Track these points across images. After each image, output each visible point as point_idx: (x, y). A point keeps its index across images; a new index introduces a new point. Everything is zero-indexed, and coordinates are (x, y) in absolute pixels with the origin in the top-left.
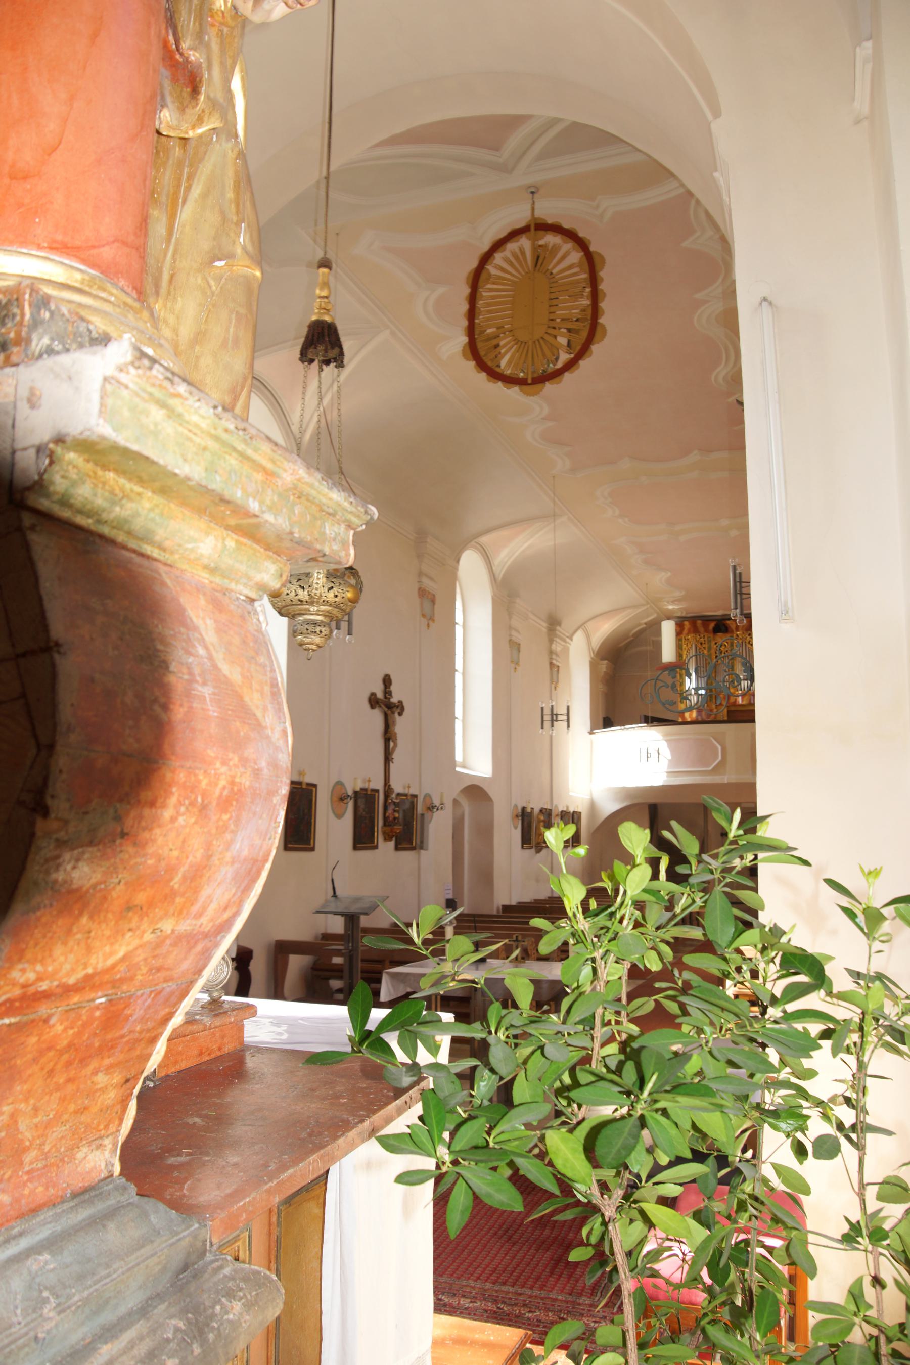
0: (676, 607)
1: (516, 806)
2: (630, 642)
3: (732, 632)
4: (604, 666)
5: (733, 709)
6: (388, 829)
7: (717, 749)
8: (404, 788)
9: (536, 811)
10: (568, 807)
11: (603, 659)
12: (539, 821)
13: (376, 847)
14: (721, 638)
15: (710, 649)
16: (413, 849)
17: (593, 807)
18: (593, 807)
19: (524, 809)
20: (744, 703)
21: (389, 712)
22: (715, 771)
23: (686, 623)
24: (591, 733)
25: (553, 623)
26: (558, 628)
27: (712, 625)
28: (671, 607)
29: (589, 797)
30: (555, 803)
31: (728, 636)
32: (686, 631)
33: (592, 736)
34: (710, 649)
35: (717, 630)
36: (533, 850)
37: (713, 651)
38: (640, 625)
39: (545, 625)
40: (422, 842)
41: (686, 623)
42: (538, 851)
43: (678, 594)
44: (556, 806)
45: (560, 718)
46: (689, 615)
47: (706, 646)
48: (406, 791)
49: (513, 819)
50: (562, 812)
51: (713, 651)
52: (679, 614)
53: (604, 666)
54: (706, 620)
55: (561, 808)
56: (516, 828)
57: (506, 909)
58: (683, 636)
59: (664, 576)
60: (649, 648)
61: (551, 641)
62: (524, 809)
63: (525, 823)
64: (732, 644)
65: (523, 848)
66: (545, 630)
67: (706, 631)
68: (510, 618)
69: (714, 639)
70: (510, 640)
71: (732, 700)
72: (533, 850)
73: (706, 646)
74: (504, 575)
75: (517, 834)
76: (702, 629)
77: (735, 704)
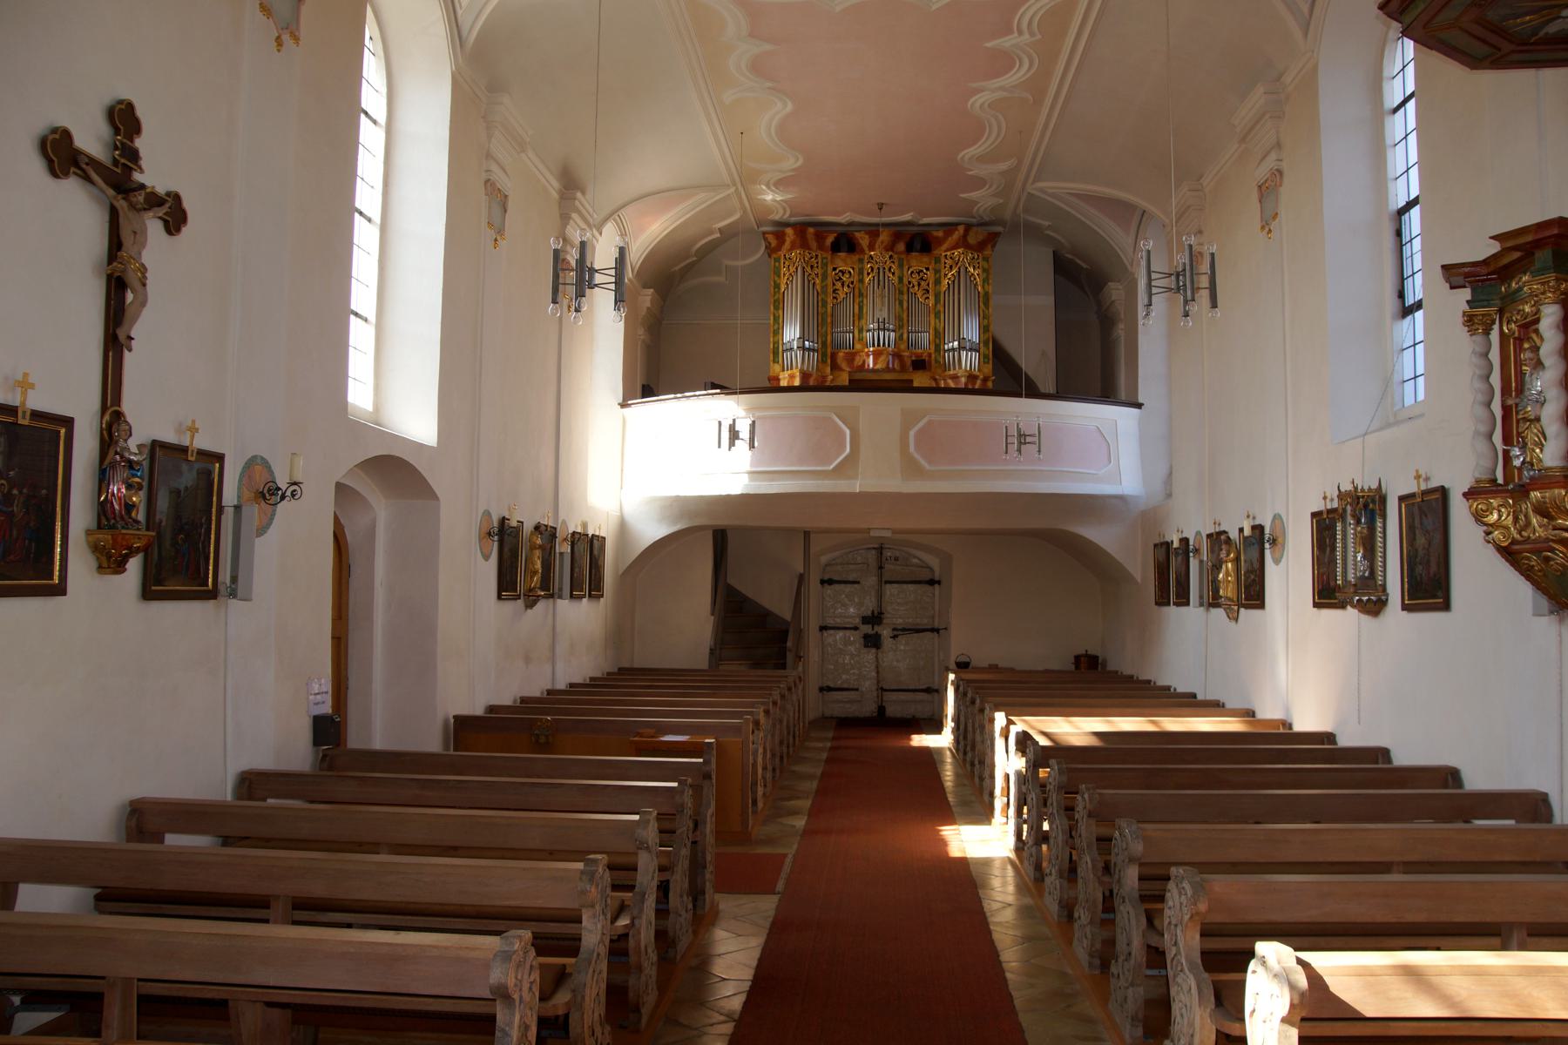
0: (779, 198)
1: (487, 514)
2: (691, 266)
3: (862, 251)
4: (647, 298)
5: (858, 376)
6: (105, 538)
7: (843, 434)
8: (179, 430)
9: (528, 527)
10: (585, 525)
11: (645, 286)
12: (533, 547)
13: (61, 590)
14: (843, 262)
15: (825, 277)
16: (212, 595)
17: (623, 527)
18: (623, 527)
19: (503, 520)
20: (878, 366)
21: (121, 204)
22: (839, 471)
23: (789, 231)
24: (623, 405)
25: (570, 185)
26: (579, 195)
27: (830, 239)
28: (769, 197)
29: (618, 514)
30: (562, 516)
31: (856, 257)
32: (787, 245)
33: (626, 411)
34: (825, 277)
35: (836, 248)
36: (520, 602)
37: (829, 280)
38: (712, 233)
39: (556, 184)
40: (234, 579)
41: (789, 231)
42: (530, 605)
43: (791, 163)
44: (564, 522)
45: (598, 278)
46: (793, 219)
47: (819, 271)
48: (185, 441)
49: (480, 540)
50: (574, 533)
51: (829, 280)
52: (777, 217)
53: (649, 298)
54: (821, 227)
55: (574, 526)
56: (486, 557)
57: (464, 728)
58: (781, 253)
59: (781, 108)
60: (721, 279)
61: (565, 218)
62: (503, 520)
63: (506, 550)
64: (861, 272)
65: (499, 597)
66: (555, 195)
67: (821, 247)
68: (490, 137)
69: (832, 262)
70: (487, 181)
71: (858, 361)
72: (520, 602)
73: (819, 271)
74: (476, 39)
75: (488, 571)
76: (814, 244)
77: (862, 368)
